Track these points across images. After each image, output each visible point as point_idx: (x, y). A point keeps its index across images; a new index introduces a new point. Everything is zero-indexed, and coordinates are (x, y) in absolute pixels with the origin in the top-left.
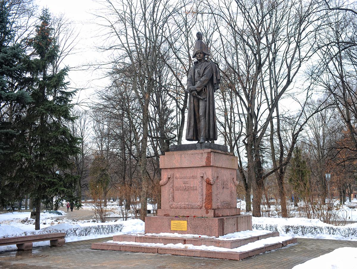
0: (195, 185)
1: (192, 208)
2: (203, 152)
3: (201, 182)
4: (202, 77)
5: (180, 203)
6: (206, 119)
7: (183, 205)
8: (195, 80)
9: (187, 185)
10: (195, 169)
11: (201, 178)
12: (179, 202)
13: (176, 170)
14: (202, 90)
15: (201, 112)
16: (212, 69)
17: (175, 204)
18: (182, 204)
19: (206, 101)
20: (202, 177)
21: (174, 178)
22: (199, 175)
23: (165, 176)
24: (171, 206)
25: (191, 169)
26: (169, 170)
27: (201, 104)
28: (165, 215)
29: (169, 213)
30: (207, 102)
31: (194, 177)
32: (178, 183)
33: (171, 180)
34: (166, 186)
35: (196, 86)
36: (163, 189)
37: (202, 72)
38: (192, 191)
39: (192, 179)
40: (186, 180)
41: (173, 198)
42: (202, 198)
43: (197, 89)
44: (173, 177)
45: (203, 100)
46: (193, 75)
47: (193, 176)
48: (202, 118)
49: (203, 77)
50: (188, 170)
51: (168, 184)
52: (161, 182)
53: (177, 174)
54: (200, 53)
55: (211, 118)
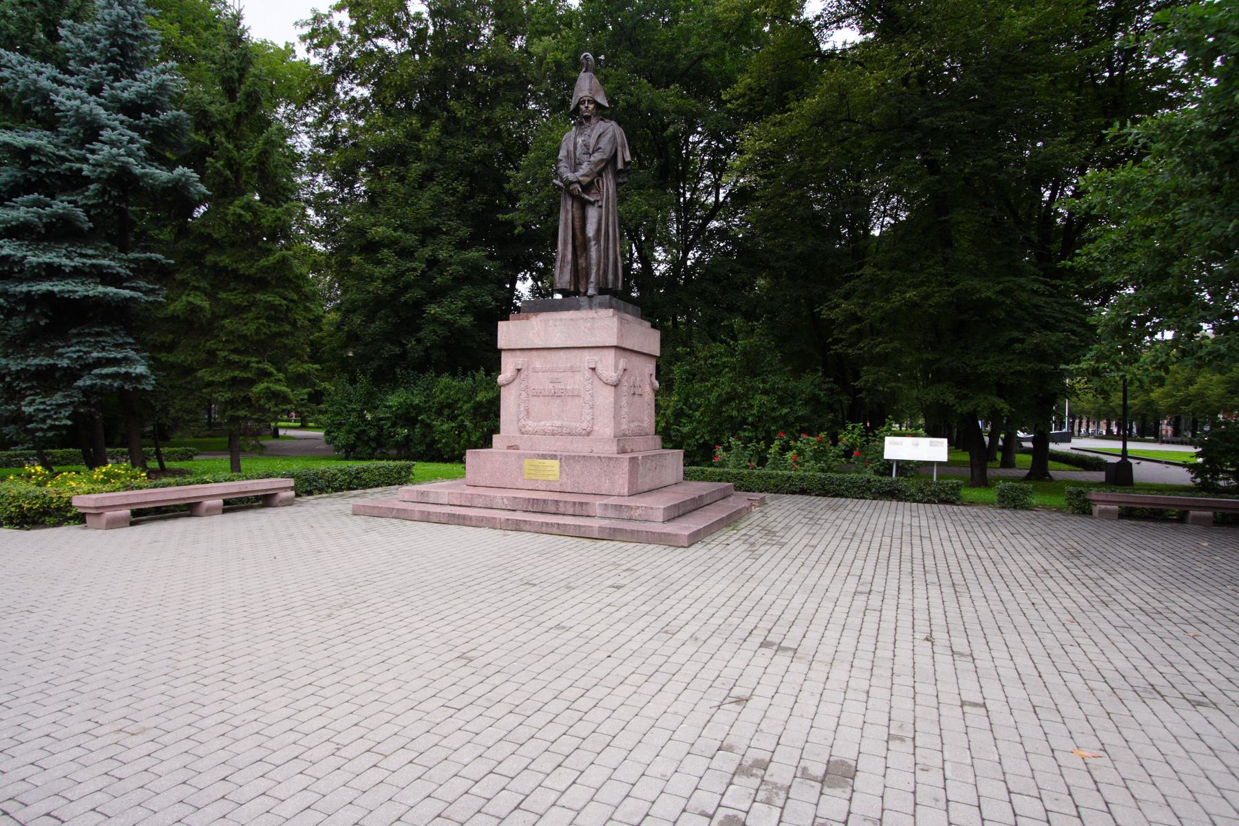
1: (569, 434)
4: (594, 152)
6: (599, 246)
10: (576, 351)
13: (535, 353)
14: (591, 183)
15: (591, 231)
16: (615, 139)
17: (531, 425)
18: (547, 424)
19: (600, 207)
20: (593, 369)
23: (508, 365)
25: (568, 351)
26: (518, 353)
27: (592, 214)
28: (509, 447)
29: (518, 442)
31: (573, 370)
33: (523, 375)
34: (512, 386)
35: (581, 172)
36: (504, 393)
37: (592, 142)
38: (569, 399)
39: (569, 374)
40: (556, 375)
46: (572, 148)
47: (572, 367)
50: (562, 353)
52: (501, 379)
53: (537, 361)
55: (611, 245)
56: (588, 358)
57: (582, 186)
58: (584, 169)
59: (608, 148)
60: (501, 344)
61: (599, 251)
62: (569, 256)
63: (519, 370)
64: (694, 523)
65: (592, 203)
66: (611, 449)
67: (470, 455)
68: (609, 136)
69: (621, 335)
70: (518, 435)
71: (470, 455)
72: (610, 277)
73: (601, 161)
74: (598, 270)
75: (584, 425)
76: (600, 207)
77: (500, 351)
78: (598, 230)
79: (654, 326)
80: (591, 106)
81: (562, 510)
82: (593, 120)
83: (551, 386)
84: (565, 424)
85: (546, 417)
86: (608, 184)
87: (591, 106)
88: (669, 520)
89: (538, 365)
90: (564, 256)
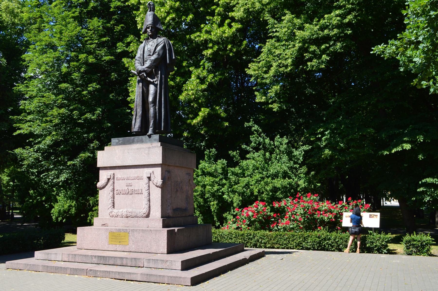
0: (141, 188)
1: (136, 217)
2: (151, 146)
5: (121, 210)
7: (125, 213)
8: (145, 59)
9: (130, 188)
11: (148, 179)
12: (120, 209)
15: (151, 99)
21: (115, 179)
22: (145, 177)
23: (103, 176)
24: (111, 214)
27: (152, 88)
30: (158, 86)
32: (120, 185)
33: (111, 182)
36: (100, 192)
41: (114, 203)
43: (146, 69)
44: (114, 178)
45: (153, 83)
48: (152, 105)
49: (154, 56)
51: (107, 187)
52: (99, 185)
53: (119, 173)
56: (147, 172)
58: (147, 64)
60: (99, 164)
61: (155, 109)
67: (79, 229)
68: (163, 44)
70: (108, 217)
71: (79, 229)
78: (155, 98)
81: (124, 263)
83: (126, 188)
84: (134, 210)
85: (125, 205)
88: (183, 269)
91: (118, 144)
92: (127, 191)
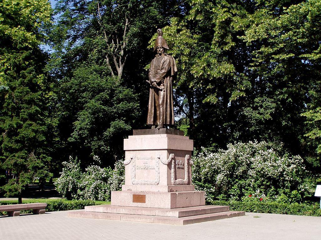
3: (158, 163)
17: (136, 181)
20: (159, 158)
23: (128, 155)
33: (133, 160)
40: (146, 161)
42: (158, 176)
43: (156, 80)
47: (151, 157)
54: (160, 48)
57: (157, 83)
59: (167, 68)
61: (163, 109)
62: (153, 111)
63: (132, 159)
64: (190, 216)
65: (161, 90)
66: (166, 190)
69: (169, 144)
72: (168, 119)
73: (164, 73)
74: (163, 117)
75: (156, 181)
76: (164, 91)
77: (125, 151)
78: (163, 101)
79: (191, 138)
80: (161, 49)
82: (163, 55)
86: (168, 81)
87: (161, 49)
89: (139, 156)
90: (151, 111)
91: (137, 134)
92: (144, 167)
